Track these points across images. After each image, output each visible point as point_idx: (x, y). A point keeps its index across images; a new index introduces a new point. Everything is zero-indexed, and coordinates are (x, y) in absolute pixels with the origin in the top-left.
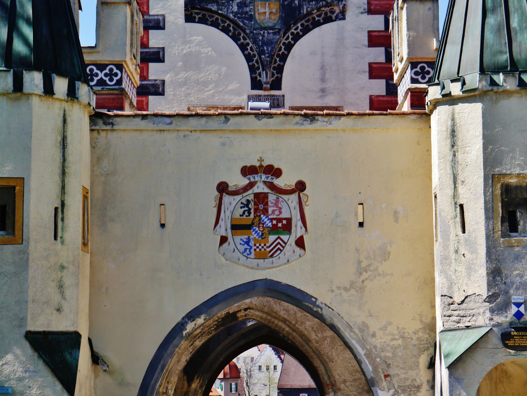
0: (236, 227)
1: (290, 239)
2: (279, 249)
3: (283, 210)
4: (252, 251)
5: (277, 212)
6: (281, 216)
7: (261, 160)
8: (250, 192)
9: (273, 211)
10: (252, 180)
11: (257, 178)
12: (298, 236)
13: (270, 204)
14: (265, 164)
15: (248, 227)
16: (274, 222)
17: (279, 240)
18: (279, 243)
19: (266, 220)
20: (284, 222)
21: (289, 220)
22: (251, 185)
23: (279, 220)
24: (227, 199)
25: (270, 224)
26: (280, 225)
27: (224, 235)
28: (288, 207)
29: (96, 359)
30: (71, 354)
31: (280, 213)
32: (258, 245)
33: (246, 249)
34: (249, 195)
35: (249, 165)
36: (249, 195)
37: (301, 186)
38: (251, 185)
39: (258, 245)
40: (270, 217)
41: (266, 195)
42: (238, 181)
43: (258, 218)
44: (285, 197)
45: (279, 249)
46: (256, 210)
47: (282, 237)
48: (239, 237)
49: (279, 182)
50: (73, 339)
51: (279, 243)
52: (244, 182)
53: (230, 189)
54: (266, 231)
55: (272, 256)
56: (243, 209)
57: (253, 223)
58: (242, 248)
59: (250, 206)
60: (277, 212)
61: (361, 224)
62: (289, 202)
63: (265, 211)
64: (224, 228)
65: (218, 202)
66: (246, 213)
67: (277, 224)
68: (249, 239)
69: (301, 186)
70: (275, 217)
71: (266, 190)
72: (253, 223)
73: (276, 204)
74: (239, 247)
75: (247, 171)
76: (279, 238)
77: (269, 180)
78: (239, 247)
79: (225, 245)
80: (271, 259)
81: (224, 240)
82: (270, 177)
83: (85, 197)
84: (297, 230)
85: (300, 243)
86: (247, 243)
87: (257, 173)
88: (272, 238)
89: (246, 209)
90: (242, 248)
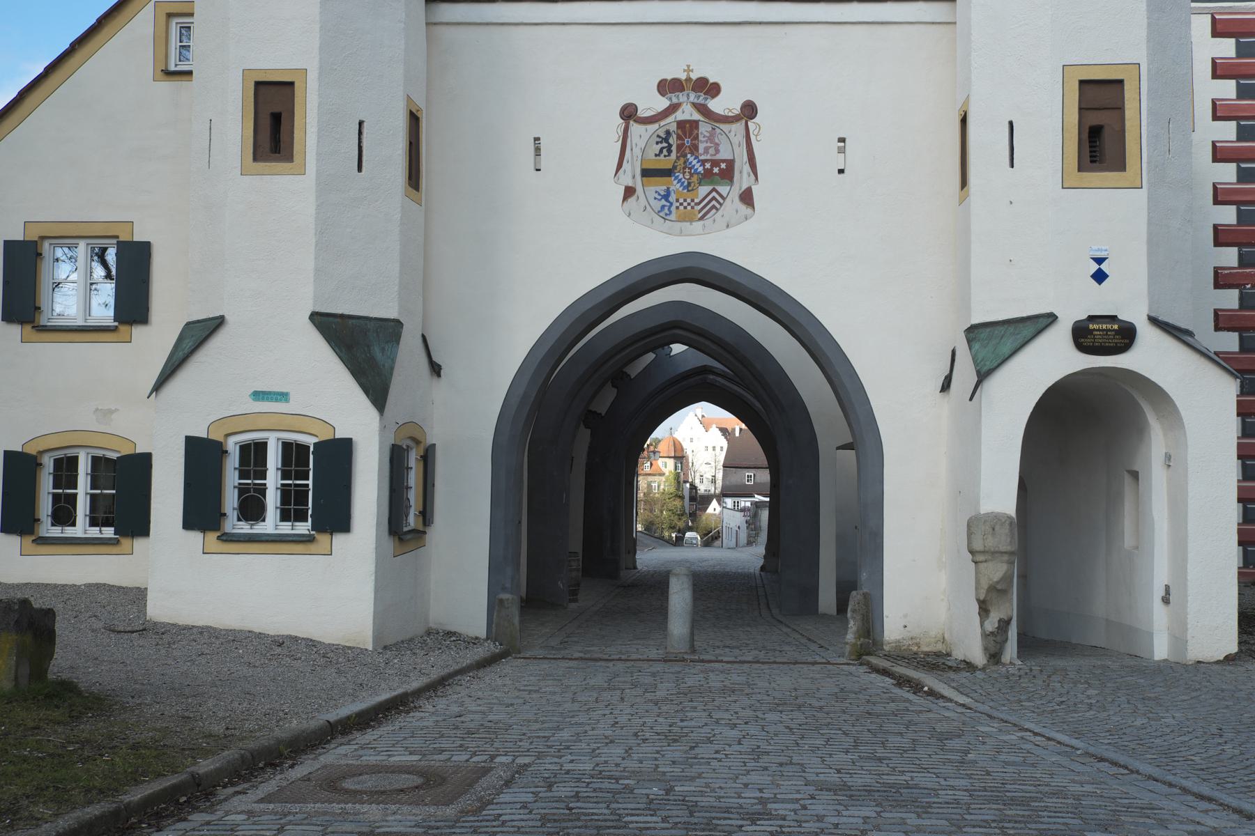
0: (646, 173)
1: (731, 193)
2: (714, 207)
3: (721, 148)
4: (673, 208)
5: (712, 151)
6: (718, 157)
7: (689, 70)
8: (671, 119)
9: (706, 150)
10: (675, 100)
11: (682, 97)
12: (744, 187)
13: (701, 138)
14: (694, 76)
15: (667, 173)
16: (708, 166)
17: (714, 194)
18: (714, 198)
19: (695, 162)
20: (723, 166)
21: (731, 163)
22: (673, 108)
23: (715, 163)
24: (635, 128)
25: (701, 169)
26: (716, 170)
27: (630, 185)
28: (729, 144)
29: (436, 369)
30: (383, 350)
31: (717, 151)
32: (681, 200)
33: (663, 207)
34: (670, 122)
35: (669, 78)
36: (670, 122)
37: (750, 110)
38: (673, 108)
39: (681, 200)
40: (702, 158)
41: (694, 124)
42: (651, 103)
43: (682, 160)
44: (725, 127)
45: (714, 207)
46: (679, 147)
47: (719, 188)
48: (653, 189)
49: (716, 105)
50: (391, 330)
51: (714, 198)
52: (662, 103)
53: (642, 113)
54: (695, 178)
55: (702, 218)
56: (660, 146)
57: (675, 167)
58: (657, 205)
59: (671, 141)
60: (712, 151)
61: (841, 171)
62: (731, 135)
63: (694, 149)
64: (631, 174)
65: (621, 133)
66: (665, 152)
67: (711, 170)
68: (668, 191)
69: (750, 110)
70: (708, 157)
71: (696, 116)
72: (675, 167)
73: (711, 138)
74: (653, 202)
75: (666, 87)
76: (714, 190)
77: (701, 100)
78: (653, 202)
79: (632, 200)
80: (701, 223)
81: (629, 192)
82: (702, 96)
83: (414, 119)
84: (743, 178)
85: (747, 198)
86: (666, 197)
87: (682, 89)
88: (703, 190)
89: (665, 145)
90: (657, 205)
